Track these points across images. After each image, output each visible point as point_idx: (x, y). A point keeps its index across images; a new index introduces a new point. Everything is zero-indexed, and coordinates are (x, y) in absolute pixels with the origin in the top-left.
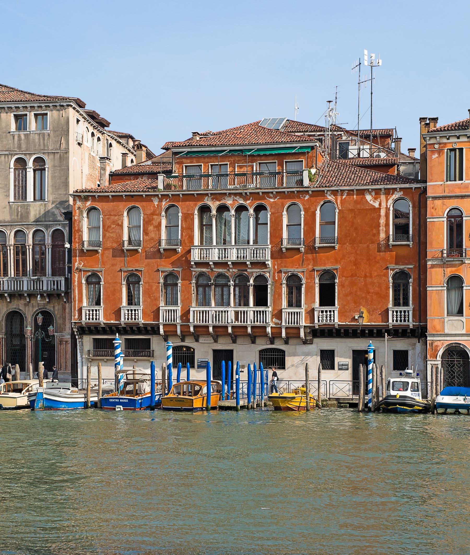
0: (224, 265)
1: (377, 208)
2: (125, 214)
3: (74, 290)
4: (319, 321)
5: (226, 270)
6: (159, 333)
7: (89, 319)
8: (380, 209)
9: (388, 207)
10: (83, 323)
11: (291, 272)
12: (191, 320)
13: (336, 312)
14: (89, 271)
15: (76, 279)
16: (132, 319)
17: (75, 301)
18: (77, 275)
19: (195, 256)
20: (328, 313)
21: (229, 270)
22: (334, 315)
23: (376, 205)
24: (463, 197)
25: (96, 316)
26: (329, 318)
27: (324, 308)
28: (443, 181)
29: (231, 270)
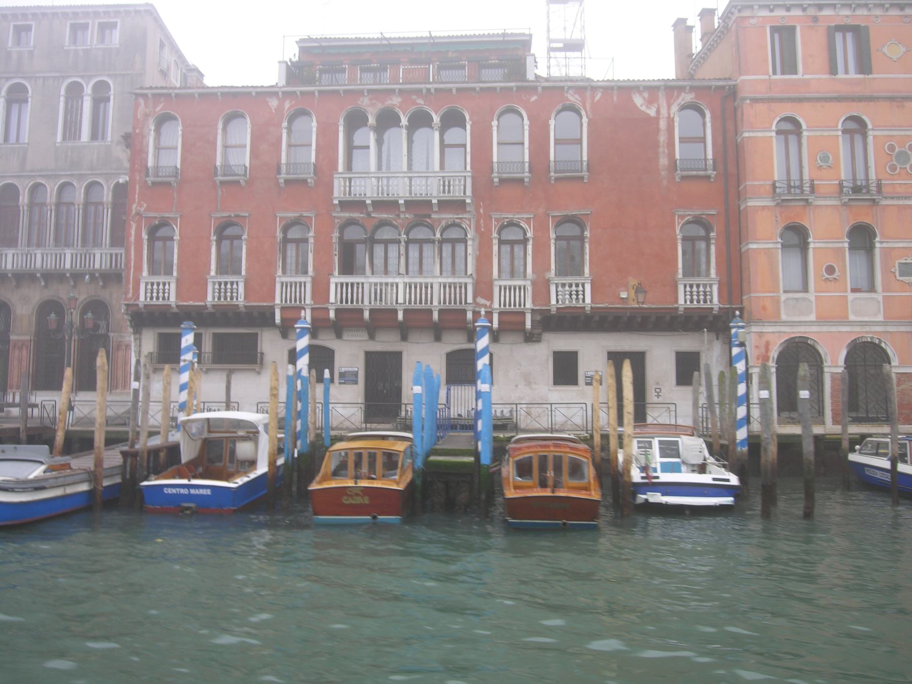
0: (389, 205)
2: (220, 125)
4: (557, 302)
6: (272, 324)
7: (152, 298)
8: (657, 119)
10: (141, 305)
12: (332, 299)
13: (588, 287)
15: (133, 232)
16: (226, 298)
18: (134, 226)
19: (339, 192)
20: (574, 288)
21: (398, 215)
22: (584, 291)
23: (652, 112)
24: (800, 100)
25: (164, 293)
26: (574, 297)
27: (568, 280)
28: (767, 74)
29: (402, 216)
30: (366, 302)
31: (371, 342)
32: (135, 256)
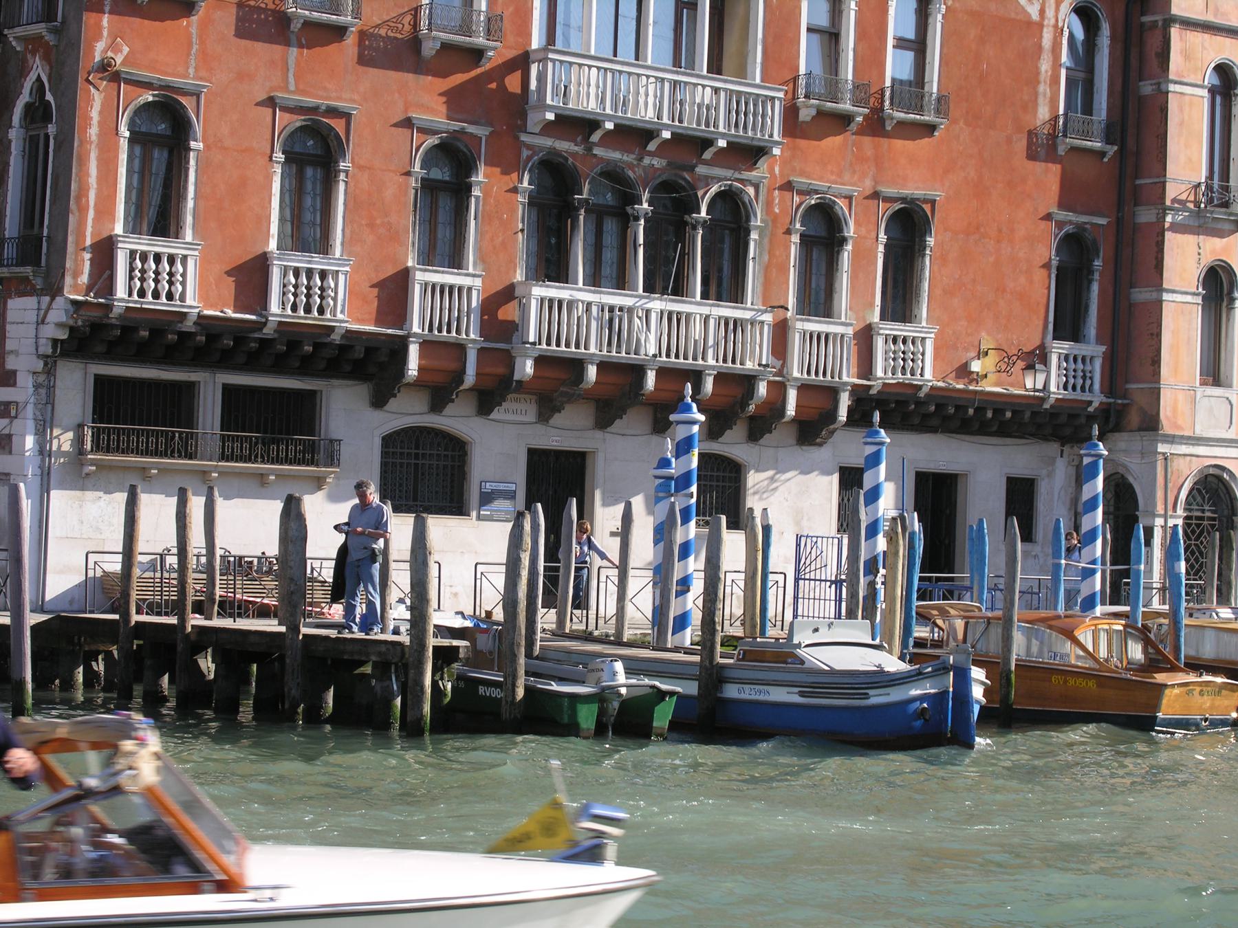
1: (1036, 23)
3: (83, 162)
5: (629, 158)
7: (142, 293)
8: (1040, 26)
9: (1060, 24)
11: (817, 192)
14: (148, 86)
15: (95, 114)
17: (83, 210)
18: (97, 98)
25: (171, 283)
30: (593, 349)
31: (540, 428)
32: (99, 178)
